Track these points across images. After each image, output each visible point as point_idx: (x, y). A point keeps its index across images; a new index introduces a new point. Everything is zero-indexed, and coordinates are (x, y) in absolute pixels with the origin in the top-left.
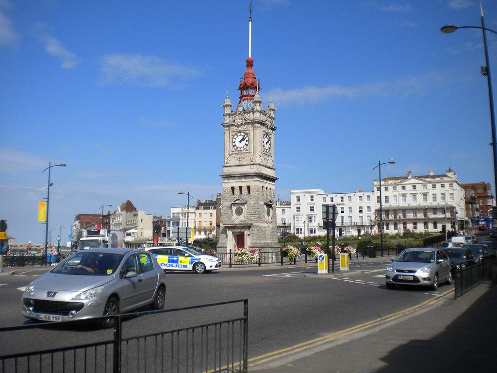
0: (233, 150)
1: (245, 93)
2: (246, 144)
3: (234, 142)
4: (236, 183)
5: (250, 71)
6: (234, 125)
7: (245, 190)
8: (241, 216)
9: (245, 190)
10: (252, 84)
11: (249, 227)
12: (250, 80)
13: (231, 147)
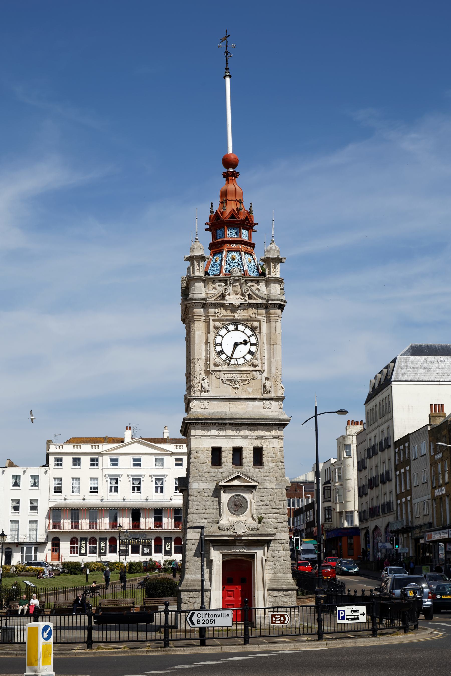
0: (218, 361)
2: (250, 352)
3: (220, 344)
4: (227, 441)
5: (231, 187)
6: (222, 305)
7: (248, 457)
8: (242, 517)
9: (248, 457)
11: (268, 542)
12: (231, 207)
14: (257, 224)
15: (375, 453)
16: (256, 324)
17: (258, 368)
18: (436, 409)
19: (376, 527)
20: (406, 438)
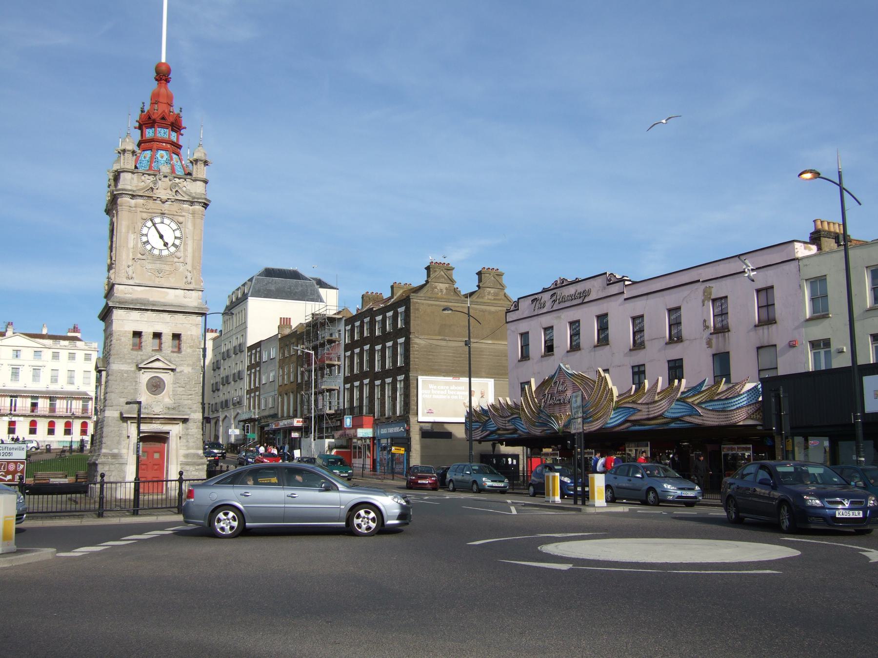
1: (149, 133)
5: (163, 90)
8: (159, 397)
10: (163, 118)
12: (160, 109)
13: (140, 245)
14: (185, 128)
15: (229, 356)
16: (181, 219)
17: (181, 260)
18: (285, 322)
19: (226, 416)
20: (259, 344)
